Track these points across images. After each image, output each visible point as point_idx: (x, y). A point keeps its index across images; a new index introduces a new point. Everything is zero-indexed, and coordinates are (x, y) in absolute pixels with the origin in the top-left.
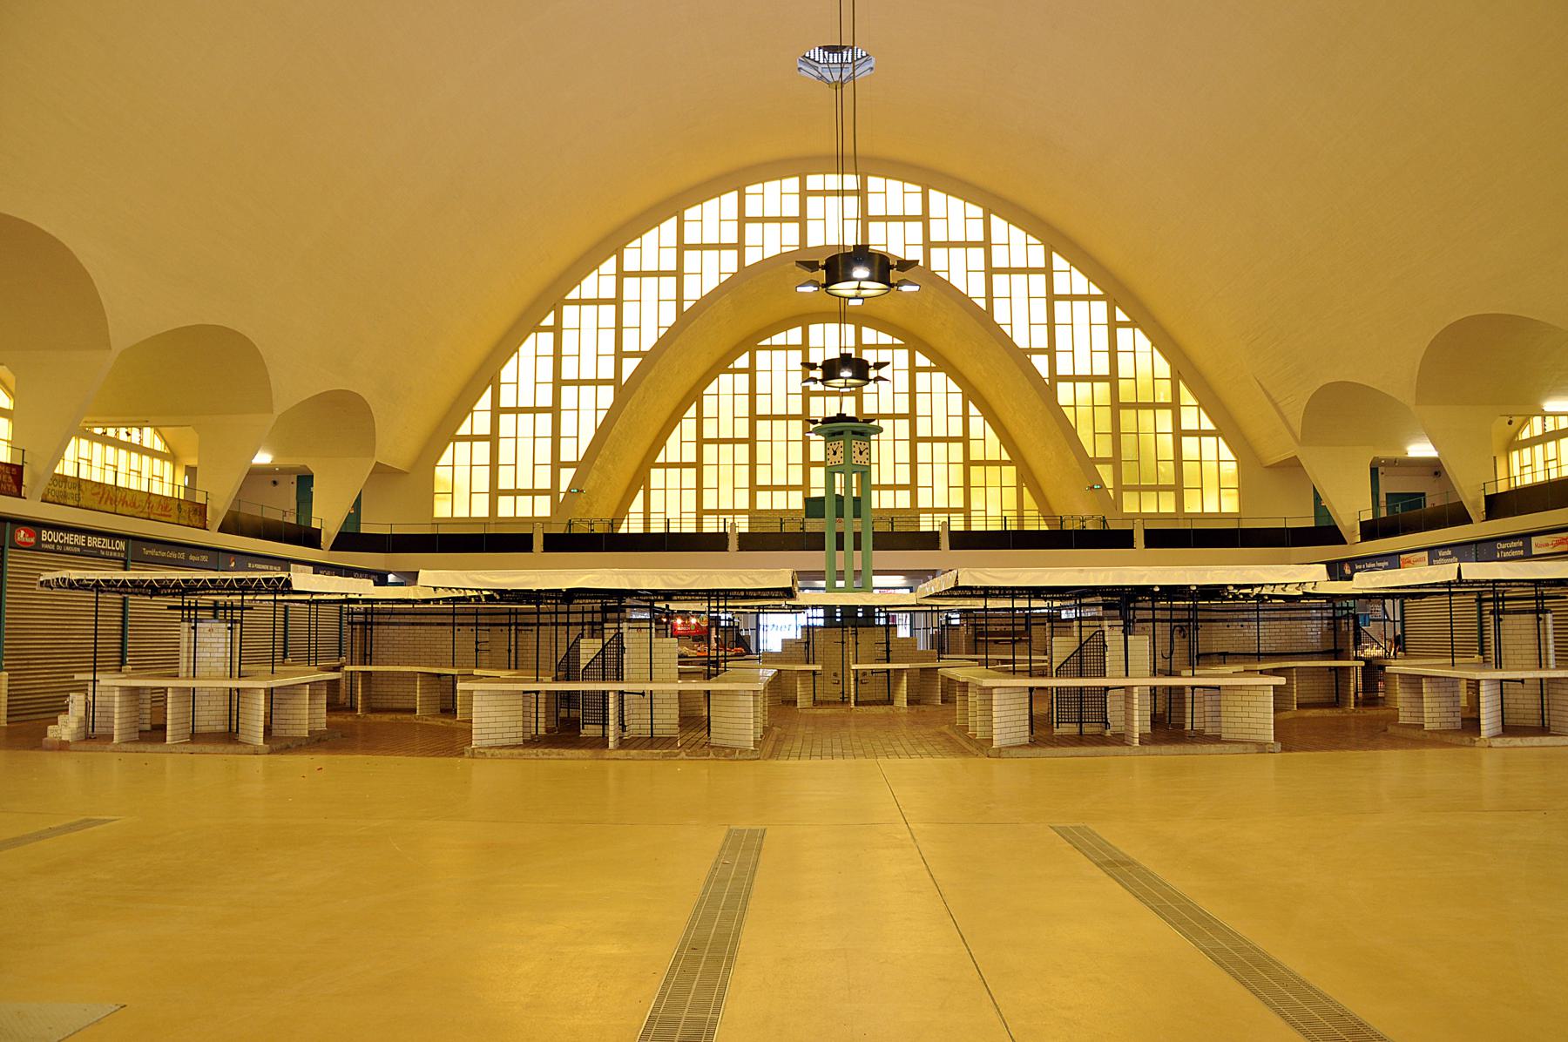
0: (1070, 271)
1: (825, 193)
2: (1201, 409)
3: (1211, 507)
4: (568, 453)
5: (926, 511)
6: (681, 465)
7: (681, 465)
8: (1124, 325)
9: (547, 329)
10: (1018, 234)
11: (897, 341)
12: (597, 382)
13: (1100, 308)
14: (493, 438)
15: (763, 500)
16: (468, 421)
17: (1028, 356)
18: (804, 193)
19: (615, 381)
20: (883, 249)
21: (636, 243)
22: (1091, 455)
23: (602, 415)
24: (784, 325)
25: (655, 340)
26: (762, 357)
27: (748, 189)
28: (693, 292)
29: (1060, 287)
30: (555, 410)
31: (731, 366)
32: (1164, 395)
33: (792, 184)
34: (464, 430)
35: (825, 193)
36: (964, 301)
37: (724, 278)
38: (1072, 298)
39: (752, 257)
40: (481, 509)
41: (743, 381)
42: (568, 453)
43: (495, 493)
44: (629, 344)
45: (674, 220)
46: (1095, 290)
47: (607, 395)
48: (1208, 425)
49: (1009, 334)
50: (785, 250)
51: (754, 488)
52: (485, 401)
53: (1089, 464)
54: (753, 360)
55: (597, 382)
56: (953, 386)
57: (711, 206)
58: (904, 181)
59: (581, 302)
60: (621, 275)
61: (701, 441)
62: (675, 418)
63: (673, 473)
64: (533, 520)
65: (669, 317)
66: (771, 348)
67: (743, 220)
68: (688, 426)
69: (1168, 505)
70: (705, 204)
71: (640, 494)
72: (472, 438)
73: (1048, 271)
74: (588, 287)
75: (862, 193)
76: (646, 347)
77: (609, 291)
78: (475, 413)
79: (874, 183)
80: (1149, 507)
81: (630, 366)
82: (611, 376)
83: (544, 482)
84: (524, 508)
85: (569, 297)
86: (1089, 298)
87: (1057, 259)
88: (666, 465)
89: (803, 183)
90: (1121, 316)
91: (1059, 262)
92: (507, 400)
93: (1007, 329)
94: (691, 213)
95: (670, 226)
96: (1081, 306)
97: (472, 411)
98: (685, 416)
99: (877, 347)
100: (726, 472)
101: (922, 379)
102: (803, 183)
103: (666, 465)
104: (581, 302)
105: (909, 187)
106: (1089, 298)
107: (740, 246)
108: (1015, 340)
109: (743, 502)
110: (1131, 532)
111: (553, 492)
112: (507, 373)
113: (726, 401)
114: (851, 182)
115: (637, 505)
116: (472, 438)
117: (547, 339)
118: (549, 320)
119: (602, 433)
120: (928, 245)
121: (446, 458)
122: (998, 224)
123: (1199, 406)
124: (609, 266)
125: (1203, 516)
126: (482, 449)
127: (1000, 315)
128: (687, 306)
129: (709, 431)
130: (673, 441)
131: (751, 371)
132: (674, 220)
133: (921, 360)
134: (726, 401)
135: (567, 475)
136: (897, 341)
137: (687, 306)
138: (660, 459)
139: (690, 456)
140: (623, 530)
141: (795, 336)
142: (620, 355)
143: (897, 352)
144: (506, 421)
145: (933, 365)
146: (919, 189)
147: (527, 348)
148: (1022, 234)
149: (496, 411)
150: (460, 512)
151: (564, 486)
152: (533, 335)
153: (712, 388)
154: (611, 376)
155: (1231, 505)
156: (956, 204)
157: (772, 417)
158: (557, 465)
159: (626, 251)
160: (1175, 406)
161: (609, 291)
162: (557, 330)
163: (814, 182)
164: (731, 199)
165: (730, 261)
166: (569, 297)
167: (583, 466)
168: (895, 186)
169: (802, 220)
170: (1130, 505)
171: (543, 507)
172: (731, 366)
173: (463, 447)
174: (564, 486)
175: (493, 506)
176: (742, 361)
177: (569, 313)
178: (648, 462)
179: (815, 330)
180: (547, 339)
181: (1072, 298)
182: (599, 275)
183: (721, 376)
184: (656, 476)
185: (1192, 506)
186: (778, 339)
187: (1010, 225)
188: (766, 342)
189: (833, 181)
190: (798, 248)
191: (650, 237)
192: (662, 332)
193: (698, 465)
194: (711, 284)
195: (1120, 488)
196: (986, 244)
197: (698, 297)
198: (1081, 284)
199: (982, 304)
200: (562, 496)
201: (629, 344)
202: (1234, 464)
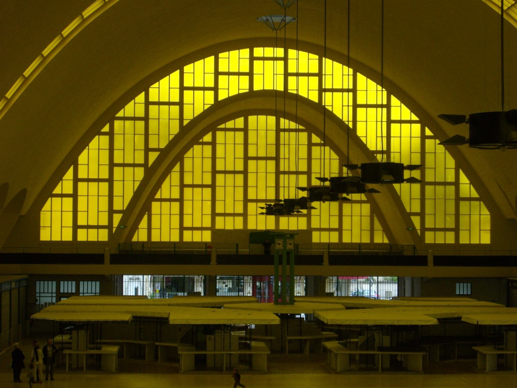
0: (401, 106)
1: (264, 59)
2: (471, 185)
3: (475, 241)
4: (118, 205)
5: (316, 230)
6: (170, 200)
7: (170, 200)
8: (429, 137)
9: (105, 134)
10: (372, 85)
11: (301, 127)
12: (134, 165)
13: (417, 127)
14: (75, 196)
15: (220, 223)
16: (60, 185)
17: (375, 155)
18: (252, 59)
19: (145, 165)
20: (295, 92)
21: (156, 85)
22: (408, 211)
23: (137, 184)
24: (233, 116)
25: (168, 142)
26: (220, 135)
27: (221, 55)
28: (189, 115)
29: (395, 116)
30: (110, 181)
31: (201, 141)
32: (451, 177)
33: (245, 52)
34: (57, 190)
35: (264, 59)
36: (339, 122)
37: (206, 107)
38: (401, 122)
39: (223, 95)
40: (68, 237)
41: (208, 149)
42: (118, 205)
43: (76, 227)
44: (153, 144)
45: (177, 72)
46: (415, 118)
47: (140, 173)
48: (475, 194)
49: (365, 142)
50: (241, 92)
51: (214, 215)
52: (69, 175)
53: (406, 216)
54: (214, 137)
55: (134, 165)
56: (334, 156)
57: (199, 64)
58: (309, 52)
59: (124, 119)
60: (148, 103)
61: (182, 186)
62: (168, 171)
63: (166, 204)
64: (98, 244)
65: (175, 129)
66: (226, 130)
67: (217, 73)
68: (175, 175)
69: (450, 238)
70: (196, 63)
71: (145, 218)
72: (62, 196)
73: (388, 106)
74: (129, 110)
75: (285, 59)
76: (163, 145)
77: (140, 112)
78: (63, 181)
79: (292, 53)
80: (440, 240)
81: (153, 157)
82: (142, 162)
83: (104, 221)
84: (93, 236)
85: (118, 115)
86: (411, 122)
87: (393, 99)
88: (161, 200)
89: (251, 53)
90: (428, 132)
91: (395, 101)
92: (82, 174)
93: (364, 140)
94: (188, 68)
95: (175, 75)
96: (406, 127)
97: (62, 180)
98: (172, 171)
99: (290, 130)
100: (198, 205)
101: (316, 151)
102: (251, 53)
103: (161, 200)
104: (124, 119)
105: (312, 56)
106: (411, 122)
107: (215, 89)
108: (369, 146)
109: (207, 223)
110: (426, 257)
111: (109, 227)
112: (82, 158)
113: (198, 162)
114: (280, 52)
115: (144, 224)
116: (62, 196)
117: (104, 140)
118: (106, 129)
119: (137, 195)
120: (322, 90)
121: (47, 206)
122: (361, 78)
123: (470, 184)
124: (141, 98)
125: (471, 246)
126: (68, 202)
127: (360, 132)
128: (185, 123)
129: (188, 180)
130: (165, 185)
131: (213, 144)
132: (177, 72)
133: (316, 139)
134: (198, 162)
135: (117, 218)
136: (301, 127)
137: (185, 123)
138: (158, 196)
139: (176, 194)
140: (135, 239)
141: (239, 122)
142: (147, 150)
143: (301, 134)
144: (82, 186)
145: (322, 142)
146: (317, 57)
147: (94, 144)
148: (374, 84)
149: (76, 180)
150: (56, 238)
151: (116, 223)
152: (97, 137)
153: (189, 154)
154: (142, 162)
155: (486, 239)
156: (338, 66)
157: (225, 172)
158: (111, 212)
159: (151, 90)
160: (456, 184)
161: (140, 112)
162: (111, 134)
163: (258, 52)
164: (210, 60)
165: (210, 98)
166: (118, 115)
167: (126, 213)
168: (303, 55)
169: (251, 74)
170: (429, 238)
171: (103, 236)
172: (201, 141)
173: (56, 201)
174: (116, 223)
175: (75, 234)
176: (208, 138)
177: (117, 124)
178: (152, 198)
179: (252, 119)
180: (104, 140)
181: (401, 122)
182: (135, 103)
183: (195, 147)
184: (155, 206)
185: (464, 240)
186: (230, 124)
187: (368, 79)
188: (222, 126)
189: (269, 52)
190: (248, 91)
191: (164, 82)
192: (171, 137)
193: (181, 200)
194: (199, 110)
195: (424, 229)
196: (354, 91)
197: (192, 118)
198: (406, 114)
199: (351, 125)
200: (114, 230)
201: (153, 144)
202: (489, 216)
